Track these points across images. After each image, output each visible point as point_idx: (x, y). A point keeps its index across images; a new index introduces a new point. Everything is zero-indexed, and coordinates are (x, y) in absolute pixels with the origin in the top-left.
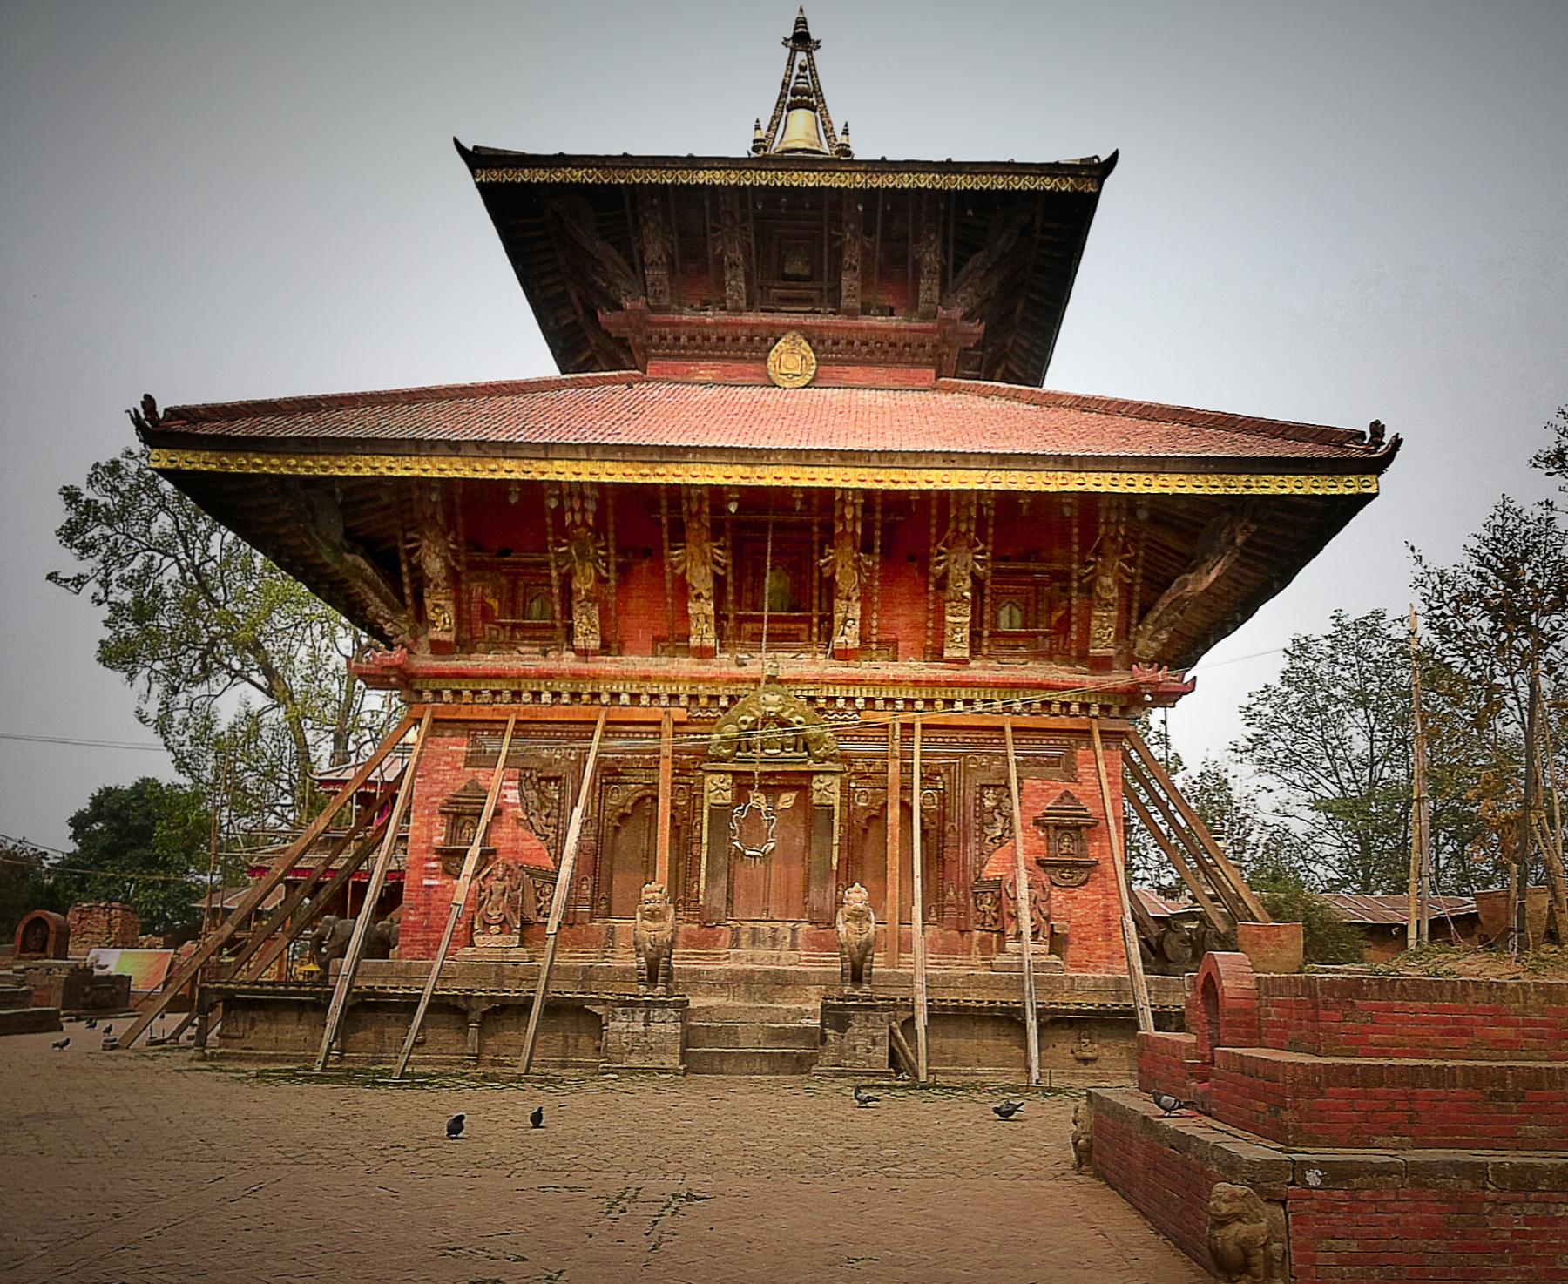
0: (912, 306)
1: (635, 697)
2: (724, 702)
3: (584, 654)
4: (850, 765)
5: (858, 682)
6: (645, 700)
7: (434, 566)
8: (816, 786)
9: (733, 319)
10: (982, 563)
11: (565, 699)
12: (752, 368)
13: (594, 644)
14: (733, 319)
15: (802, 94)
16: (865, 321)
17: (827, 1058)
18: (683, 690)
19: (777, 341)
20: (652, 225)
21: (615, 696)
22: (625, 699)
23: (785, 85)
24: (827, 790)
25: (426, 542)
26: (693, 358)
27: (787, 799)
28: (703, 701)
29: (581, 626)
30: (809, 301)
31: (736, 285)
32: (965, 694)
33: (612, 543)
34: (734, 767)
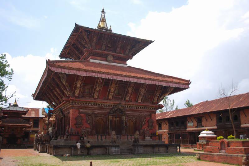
0: (124, 54)
1: (101, 105)
2: (112, 106)
3: (95, 99)
4: (126, 115)
5: (129, 104)
6: (103, 105)
7: (78, 85)
8: (122, 117)
9: (102, 52)
10: (145, 91)
11: (93, 105)
12: (104, 59)
13: (97, 97)
14: (102, 52)
15: (103, 20)
16: (119, 54)
17: (136, 152)
18: (108, 104)
19: (108, 55)
20: (95, 38)
21: (99, 105)
22: (100, 105)
23: (101, 18)
24: (124, 118)
25: (78, 82)
26: (97, 56)
27: (118, 119)
28: (110, 106)
29: (95, 95)
30: (111, 50)
31: (104, 47)
32: (140, 106)
33: (103, 85)
34: (112, 115)
